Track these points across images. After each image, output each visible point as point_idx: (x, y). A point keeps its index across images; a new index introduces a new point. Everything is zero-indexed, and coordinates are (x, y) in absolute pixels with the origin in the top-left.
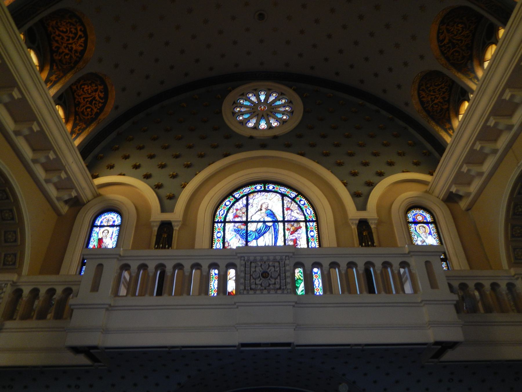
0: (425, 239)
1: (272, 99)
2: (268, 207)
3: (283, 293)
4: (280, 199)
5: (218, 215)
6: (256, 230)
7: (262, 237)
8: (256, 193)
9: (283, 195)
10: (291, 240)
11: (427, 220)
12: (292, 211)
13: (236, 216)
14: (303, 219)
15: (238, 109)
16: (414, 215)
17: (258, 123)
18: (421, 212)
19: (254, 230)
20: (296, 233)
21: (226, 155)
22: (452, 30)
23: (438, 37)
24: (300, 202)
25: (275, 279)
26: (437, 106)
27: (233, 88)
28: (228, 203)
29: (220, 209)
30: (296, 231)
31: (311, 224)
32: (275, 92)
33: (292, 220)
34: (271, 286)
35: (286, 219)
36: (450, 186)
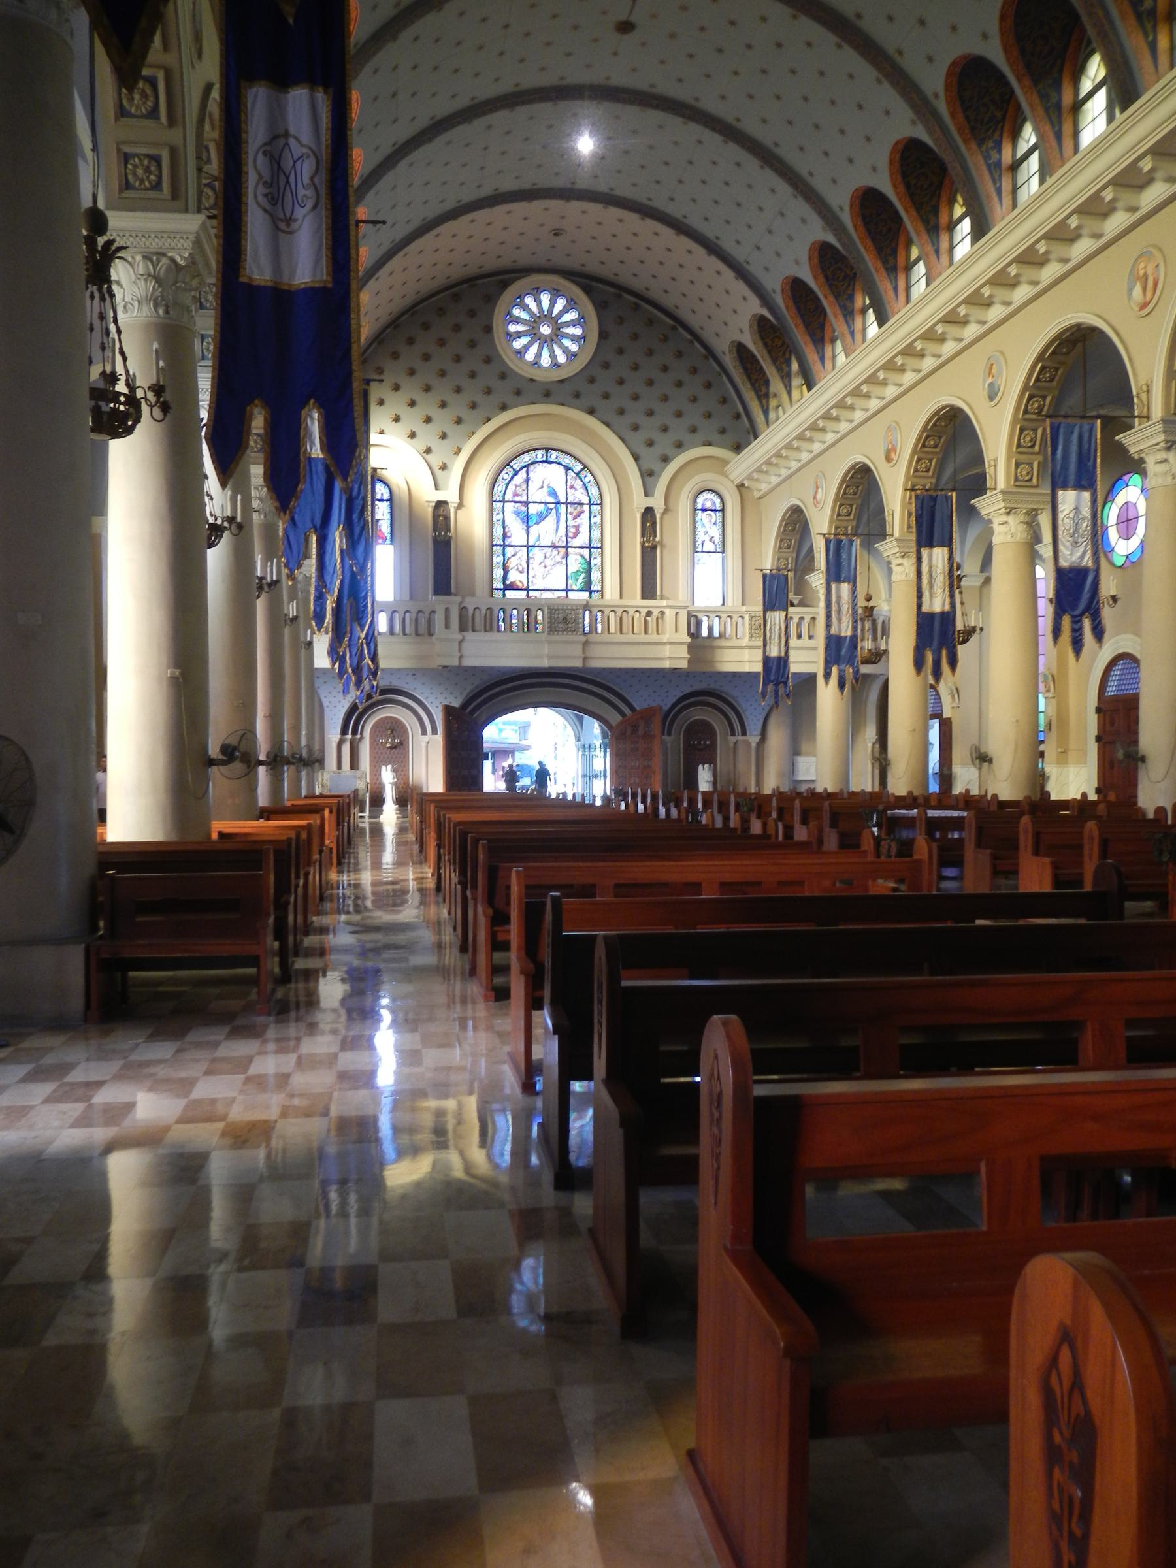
9: (567, 468)
10: (574, 526)
12: (576, 490)
13: (515, 495)
17: (539, 355)
19: (535, 512)
21: (504, 408)
27: (505, 285)
28: (506, 476)
36: (743, 480)
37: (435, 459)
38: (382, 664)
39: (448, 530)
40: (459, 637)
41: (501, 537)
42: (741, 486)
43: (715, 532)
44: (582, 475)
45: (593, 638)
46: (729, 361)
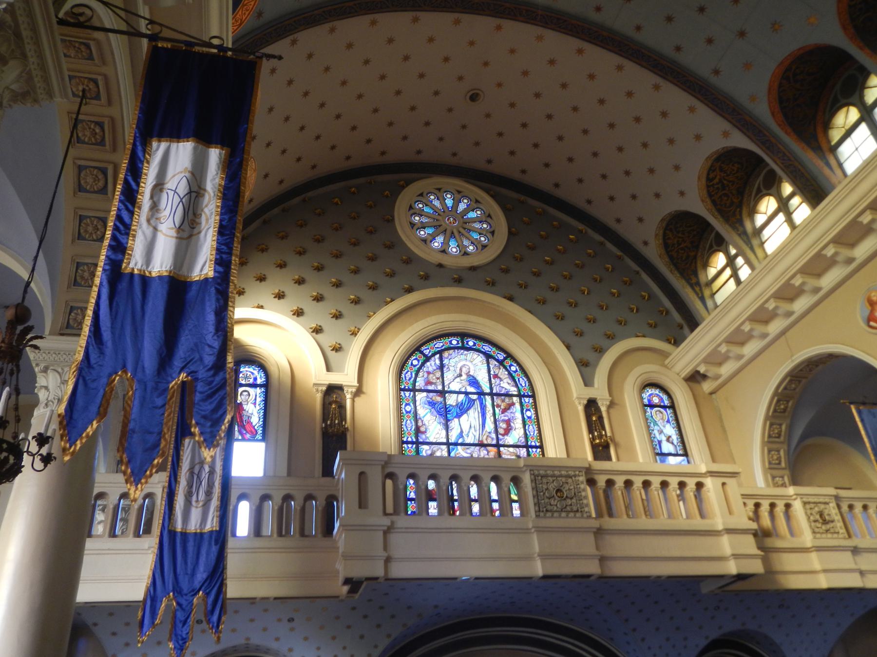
0: (662, 428)
1: (462, 206)
2: (469, 372)
3: (582, 517)
4: (485, 362)
5: (404, 379)
6: (457, 405)
7: (465, 416)
8: (452, 351)
9: (488, 356)
10: (503, 421)
11: (664, 403)
13: (428, 383)
14: (516, 393)
15: (417, 218)
16: (650, 395)
18: (657, 392)
19: (454, 404)
20: (508, 411)
21: (410, 290)
22: (726, 169)
23: (708, 174)
24: (510, 368)
25: (571, 498)
26: (683, 252)
27: (408, 183)
28: (415, 362)
29: (406, 371)
30: (509, 409)
31: (527, 400)
32: (467, 197)
33: (502, 392)
34: (568, 508)
35: (494, 391)
36: (698, 365)
37: (328, 340)
38: (233, 590)
39: (343, 417)
40: (386, 521)
41: (413, 432)
42: (695, 378)
43: (670, 430)
44: (507, 365)
45: (609, 523)
46: (654, 253)
